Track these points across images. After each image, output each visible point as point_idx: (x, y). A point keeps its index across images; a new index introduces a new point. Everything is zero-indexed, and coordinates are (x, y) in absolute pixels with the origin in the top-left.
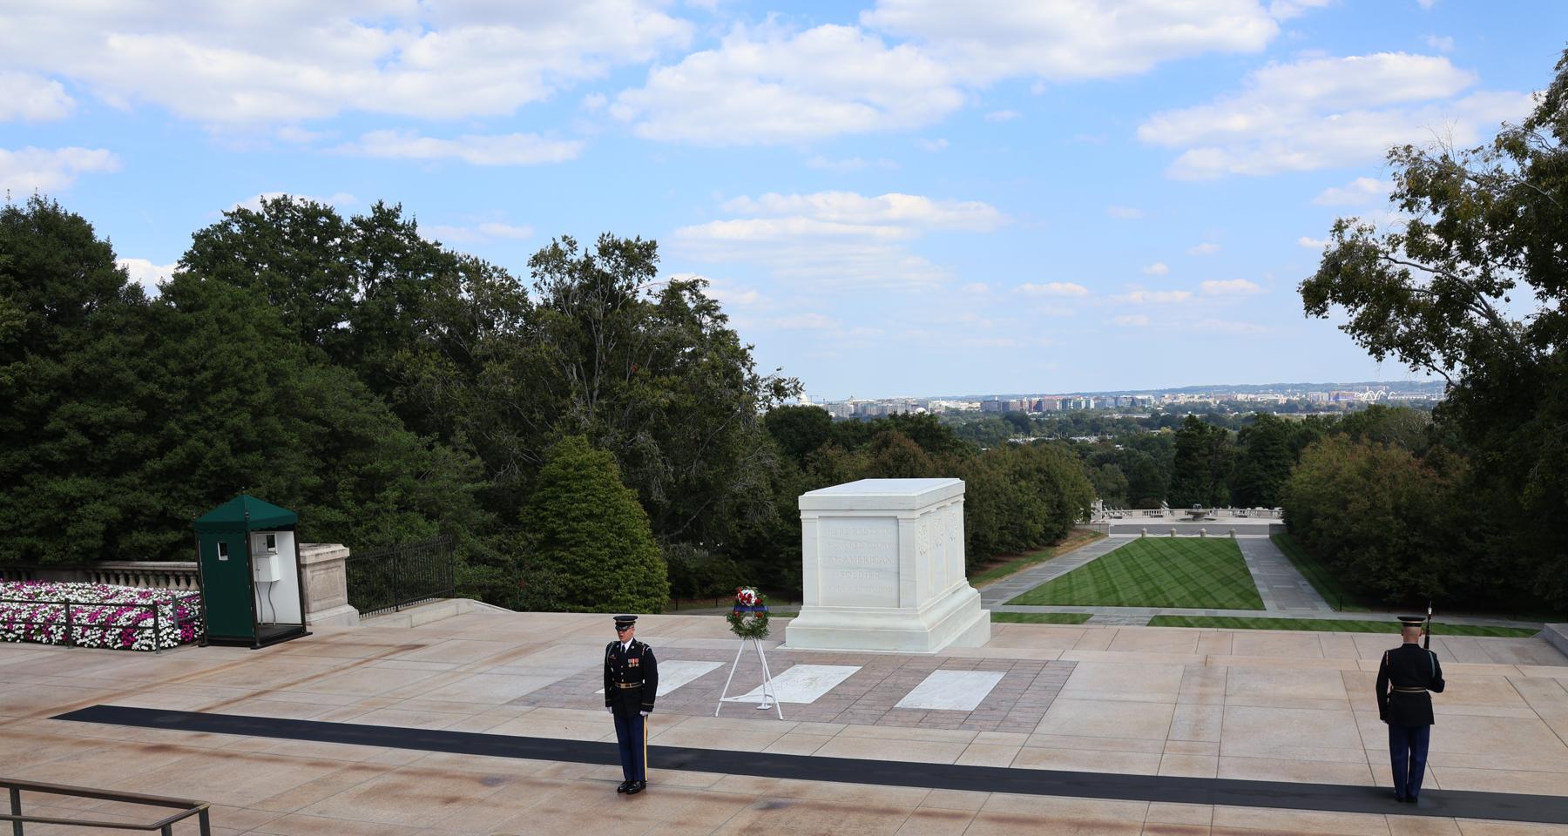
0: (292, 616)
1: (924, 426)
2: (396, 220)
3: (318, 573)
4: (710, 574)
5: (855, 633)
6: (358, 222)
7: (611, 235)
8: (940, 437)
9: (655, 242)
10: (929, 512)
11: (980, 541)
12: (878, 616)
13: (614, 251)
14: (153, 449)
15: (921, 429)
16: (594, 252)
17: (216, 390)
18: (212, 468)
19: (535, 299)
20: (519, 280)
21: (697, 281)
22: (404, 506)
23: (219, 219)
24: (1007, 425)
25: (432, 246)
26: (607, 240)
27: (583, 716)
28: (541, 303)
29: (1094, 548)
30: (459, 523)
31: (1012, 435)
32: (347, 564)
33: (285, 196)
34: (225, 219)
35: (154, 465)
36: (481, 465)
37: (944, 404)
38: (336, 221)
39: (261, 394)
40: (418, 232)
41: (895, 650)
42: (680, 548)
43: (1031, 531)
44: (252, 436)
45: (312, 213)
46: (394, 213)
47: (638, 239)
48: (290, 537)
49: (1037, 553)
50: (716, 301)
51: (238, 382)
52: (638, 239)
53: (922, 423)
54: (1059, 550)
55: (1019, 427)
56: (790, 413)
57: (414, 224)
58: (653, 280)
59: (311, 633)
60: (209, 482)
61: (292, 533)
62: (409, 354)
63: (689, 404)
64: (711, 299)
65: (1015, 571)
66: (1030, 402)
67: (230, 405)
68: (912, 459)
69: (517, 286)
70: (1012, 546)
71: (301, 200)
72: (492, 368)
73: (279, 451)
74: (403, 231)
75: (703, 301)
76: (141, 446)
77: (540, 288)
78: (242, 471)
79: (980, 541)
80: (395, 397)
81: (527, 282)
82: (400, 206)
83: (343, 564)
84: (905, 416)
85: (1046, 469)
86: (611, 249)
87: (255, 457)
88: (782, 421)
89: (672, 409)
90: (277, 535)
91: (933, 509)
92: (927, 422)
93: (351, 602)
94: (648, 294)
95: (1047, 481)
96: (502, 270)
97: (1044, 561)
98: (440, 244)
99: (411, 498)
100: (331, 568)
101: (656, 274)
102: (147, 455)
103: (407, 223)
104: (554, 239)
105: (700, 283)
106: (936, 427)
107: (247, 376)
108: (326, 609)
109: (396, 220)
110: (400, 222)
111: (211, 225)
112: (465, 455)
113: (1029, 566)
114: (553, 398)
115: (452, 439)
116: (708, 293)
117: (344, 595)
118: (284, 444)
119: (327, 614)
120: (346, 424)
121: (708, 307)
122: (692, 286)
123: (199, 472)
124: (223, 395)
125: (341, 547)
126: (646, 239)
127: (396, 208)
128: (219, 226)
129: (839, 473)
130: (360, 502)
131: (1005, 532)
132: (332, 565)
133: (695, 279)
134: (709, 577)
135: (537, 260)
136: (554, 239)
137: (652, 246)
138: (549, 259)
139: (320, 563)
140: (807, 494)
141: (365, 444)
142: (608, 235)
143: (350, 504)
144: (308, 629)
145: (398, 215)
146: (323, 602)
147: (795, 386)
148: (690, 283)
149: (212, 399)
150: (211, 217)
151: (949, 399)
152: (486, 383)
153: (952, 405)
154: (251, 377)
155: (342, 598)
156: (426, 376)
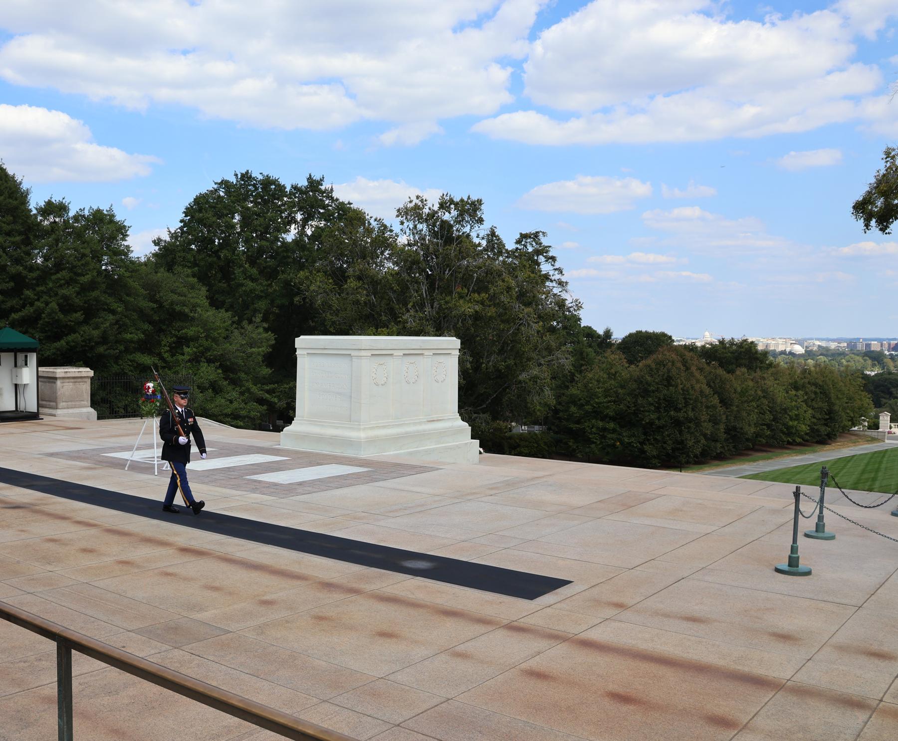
0: (32, 407)
1: (742, 350)
2: (320, 187)
3: (67, 384)
4: (518, 441)
5: (320, 439)
6: (295, 187)
7: (449, 195)
8: (757, 359)
9: (481, 200)
10: (391, 355)
11: (738, 432)
12: (337, 428)
13: (449, 206)
14: (18, 306)
15: (741, 352)
16: (436, 208)
17: (57, 272)
18: (46, 320)
19: (403, 240)
20: (391, 226)
21: (537, 233)
22: (195, 360)
23: (211, 186)
24: (865, 360)
25: (346, 205)
26: (446, 198)
27: (58, 462)
28: (406, 243)
29: (865, 449)
30: (246, 374)
31: (869, 369)
32: (91, 380)
33: (248, 171)
34: (216, 186)
35: (15, 316)
36: (273, 338)
37: (818, 343)
38: (281, 188)
39: (87, 276)
40: (335, 195)
41: (342, 453)
42: (480, 417)
43: (796, 430)
44: (77, 301)
45: (268, 182)
46: (319, 183)
47: (469, 198)
48: (33, 358)
49: (806, 448)
50: (550, 247)
51: (72, 269)
52: (469, 198)
53: (743, 348)
54: (827, 447)
55: (876, 362)
56: (641, 336)
57: (332, 190)
58: (482, 227)
59: (43, 419)
60: (47, 329)
61: (35, 354)
62: (307, 274)
63: (489, 315)
64: (546, 245)
65: (772, 459)
66: (889, 344)
67: (63, 282)
68: (670, 364)
69: (391, 231)
70: (776, 440)
71: (261, 173)
72: (352, 284)
73: (103, 314)
74: (324, 195)
75: (540, 247)
76: (9, 304)
77: (405, 233)
78: (69, 323)
79: (738, 432)
80: (295, 302)
81: (397, 228)
82: (323, 178)
83: (89, 381)
84: (732, 343)
85: (820, 383)
86: (448, 205)
87: (79, 316)
88: (635, 342)
89: (477, 317)
90: (29, 355)
91: (401, 353)
92: (747, 346)
93: (91, 407)
94: (477, 237)
95: (821, 393)
96: (380, 220)
97: (806, 454)
98: (352, 204)
99: (209, 354)
100: (80, 382)
101: (484, 223)
102: (13, 310)
103: (327, 188)
104: (410, 198)
105: (541, 233)
106: (754, 351)
107: (79, 264)
108: (72, 408)
109: (320, 187)
110: (323, 188)
111: (207, 191)
112: (261, 330)
113: (788, 456)
114: (397, 306)
115: (254, 319)
116: (545, 241)
117: (87, 401)
118: (113, 312)
119: (71, 411)
120: (172, 303)
121: (542, 251)
122: (536, 235)
123: (41, 322)
124: (59, 275)
125: (88, 369)
126: (474, 198)
127: (321, 179)
128: (212, 191)
129: (616, 373)
130: (173, 355)
131: (765, 427)
132: (79, 380)
133: (537, 231)
134: (517, 443)
135: (399, 212)
136: (410, 198)
137: (480, 202)
138: (412, 212)
139: (68, 378)
140: (302, 337)
141: (183, 317)
142: (447, 194)
143: (166, 355)
144: (41, 416)
145: (322, 183)
146: (70, 403)
147: (577, 305)
148: (533, 234)
149: (54, 277)
150: (206, 186)
151: (822, 340)
152: (348, 294)
153: (823, 344)
154: (82, 265)
155: (86, 403)
156: (312, 288)
